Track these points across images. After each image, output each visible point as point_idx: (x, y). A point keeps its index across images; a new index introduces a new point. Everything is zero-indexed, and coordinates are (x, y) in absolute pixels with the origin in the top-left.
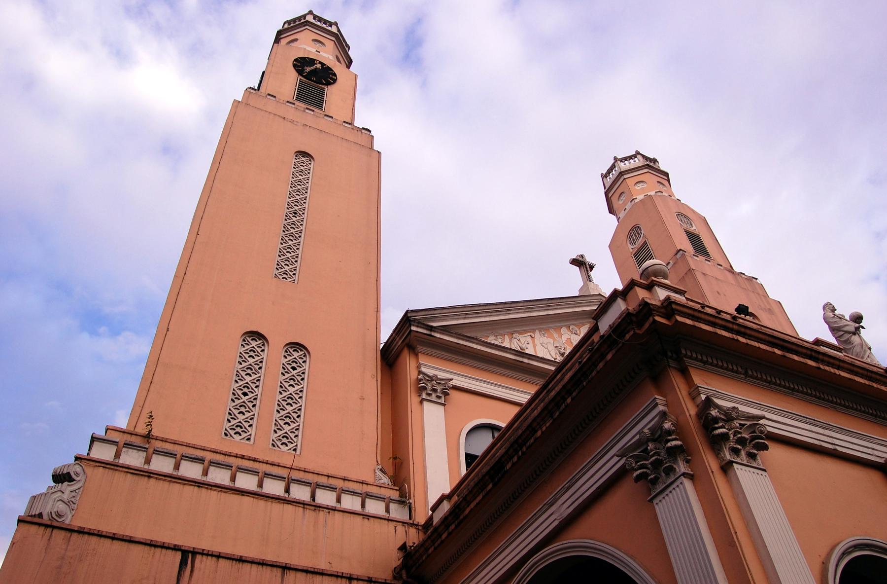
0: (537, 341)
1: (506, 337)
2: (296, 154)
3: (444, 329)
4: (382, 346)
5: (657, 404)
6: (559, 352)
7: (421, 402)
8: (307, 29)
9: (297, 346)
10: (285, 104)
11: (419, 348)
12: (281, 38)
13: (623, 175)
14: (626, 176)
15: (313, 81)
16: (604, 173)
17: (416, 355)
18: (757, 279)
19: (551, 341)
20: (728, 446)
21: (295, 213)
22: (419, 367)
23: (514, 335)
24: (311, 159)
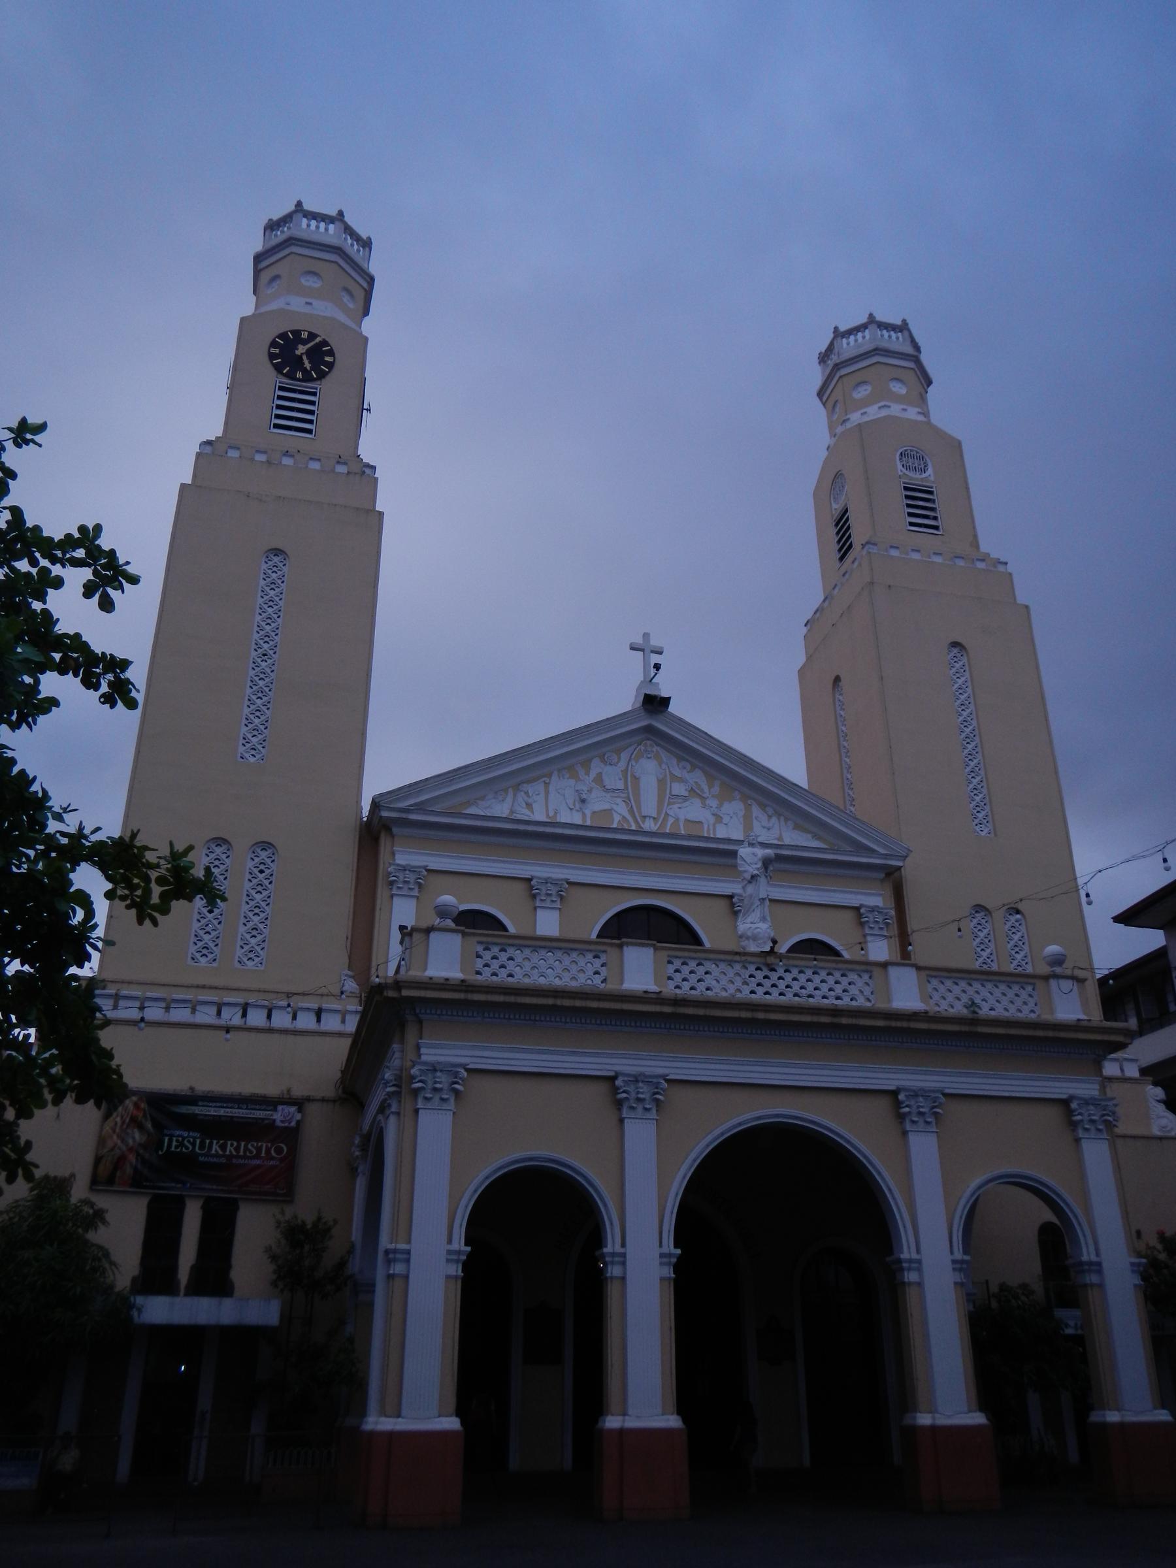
0: (551, 788)
1: (511, 790)
2: (266, 554)
3: (420, 807)
4: (365, 819)
5: (394, 1052)
6: (580, 798)
7: (392, 896)
8: (292, 253)
9: (266, 845)
10: (252, 459)
11: (395, 830)
12: (261, 270)
13: (839, 369)
14: (843, 372)
15: (299, 380)
16: (823, 351)
17: (392, 836)
18: (1006, 563)
19: (572, 782)
20: (422, 1095)
21: (264, 655)
22: (393, 854)
23: (520, 787)
24: (287, 559)
